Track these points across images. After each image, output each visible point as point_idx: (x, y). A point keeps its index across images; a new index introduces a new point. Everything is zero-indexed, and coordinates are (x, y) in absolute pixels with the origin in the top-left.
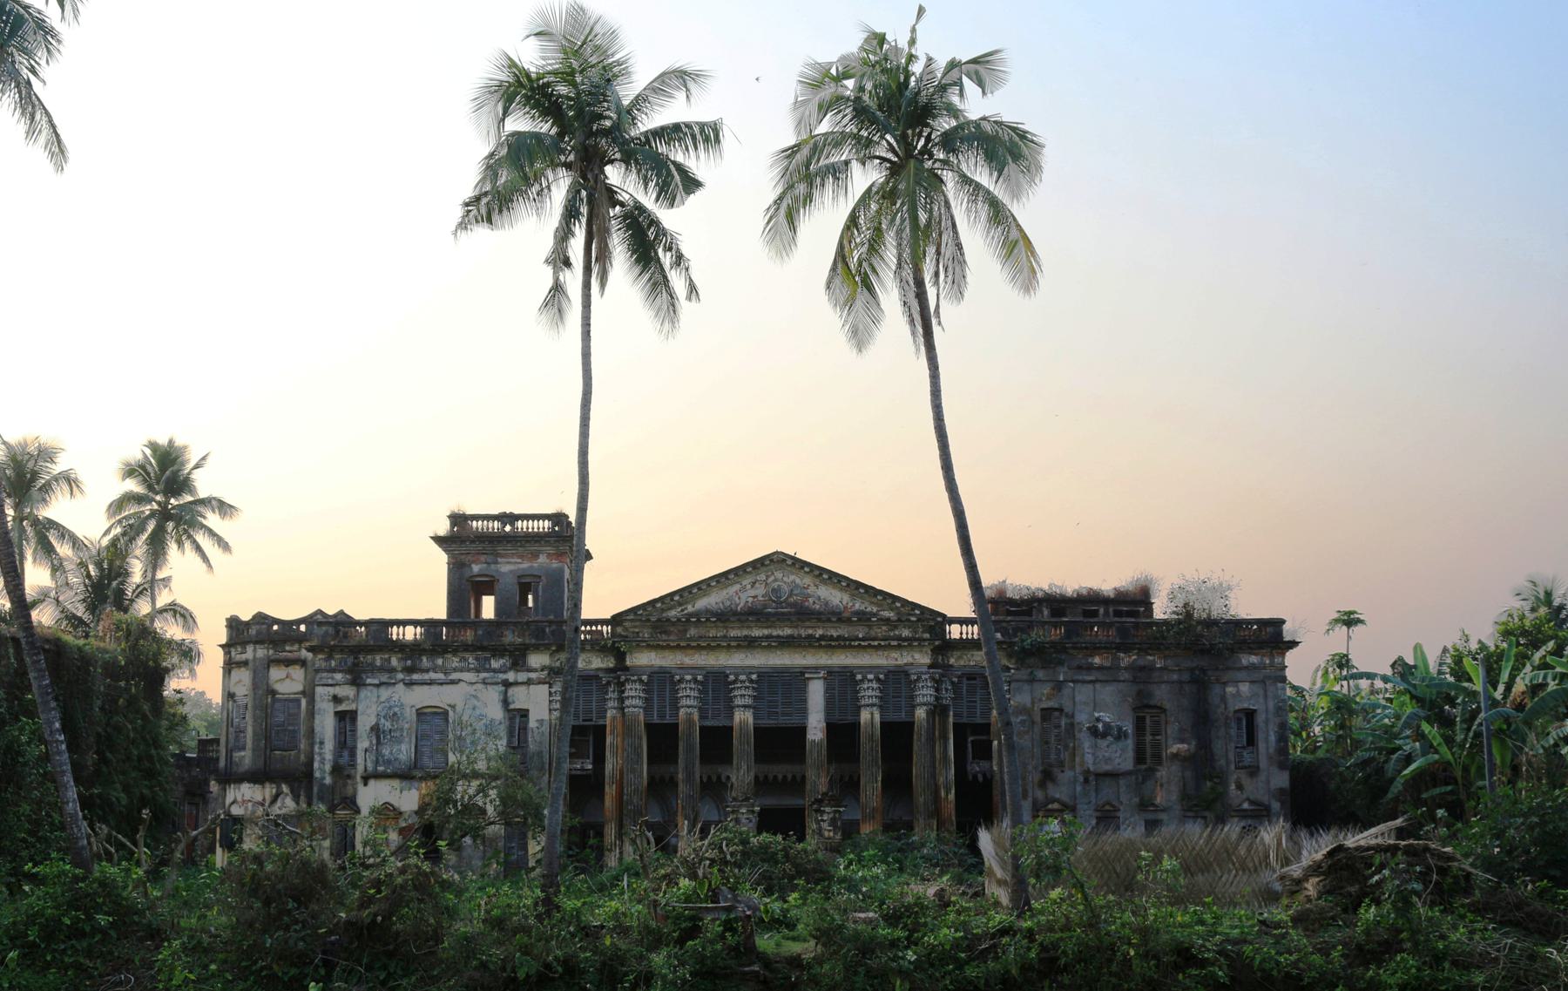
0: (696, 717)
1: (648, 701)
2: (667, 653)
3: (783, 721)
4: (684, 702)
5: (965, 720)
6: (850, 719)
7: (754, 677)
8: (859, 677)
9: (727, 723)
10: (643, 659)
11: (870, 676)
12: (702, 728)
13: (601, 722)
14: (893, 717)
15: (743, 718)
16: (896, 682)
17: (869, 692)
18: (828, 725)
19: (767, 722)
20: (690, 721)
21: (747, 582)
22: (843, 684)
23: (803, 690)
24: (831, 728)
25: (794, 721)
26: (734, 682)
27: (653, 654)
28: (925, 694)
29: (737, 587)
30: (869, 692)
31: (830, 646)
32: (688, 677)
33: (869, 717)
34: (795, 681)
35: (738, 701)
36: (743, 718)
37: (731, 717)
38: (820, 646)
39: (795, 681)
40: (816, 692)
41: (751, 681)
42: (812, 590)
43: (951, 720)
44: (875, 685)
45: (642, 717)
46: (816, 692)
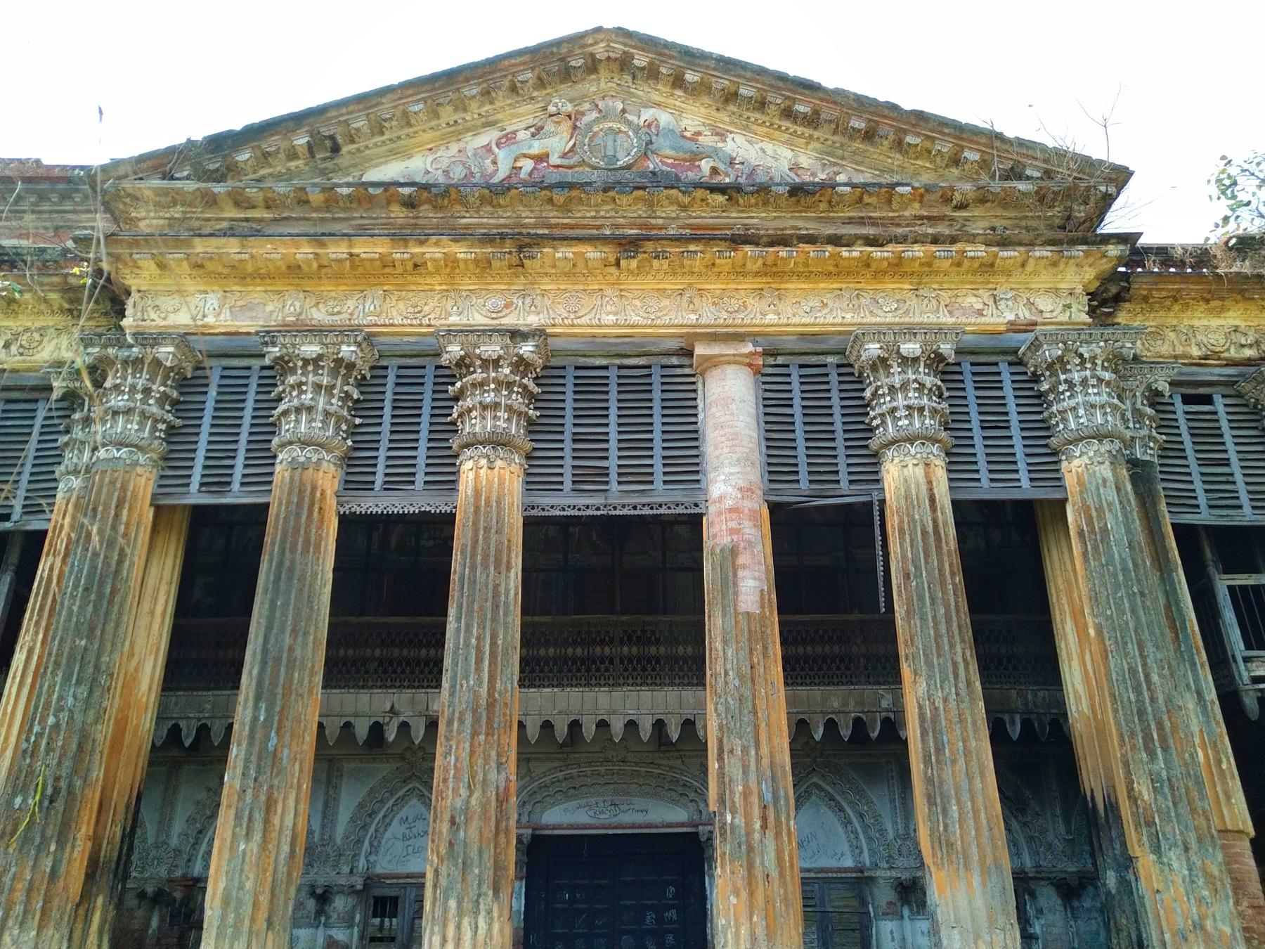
0: (329, 478)
1: (177, 441)
2: (256, 293)
3: (617, 499)
4: (287, 427)
5: (1205, 517)
6: (846, 492)
7: (527, 349)
8: (873, 349)
9: (433, 503)
10: (182, 306)
11: (911, 348)
12: (347, 521)
13: (35, 525)
14: (986, 488)
15: (490, 487)
16: (989, 383)
17: (904, 404)
18: (774, 508)
19: (565, 501)
20: (304, 496)
21: (520, 118)
22: (815, 390)
23: (683, 406)
24: (789, 525)
25: (662, 497)
26: (463, 364)
27: (213, 301)
28: (1085, 405)
29: (488, 137)
30: (904, 404)
31: (773, 272)
32: (311, 349)
33: (912, 480)
34: (657, 384)
35: (476, 425)
36: (490, 487)
37: (450, 485)
38: (739, 272)
39: (657, 384)
40: (729, 410)
41: (521, 365)
42: (707, 140)
43: (1167, 520)
44: (929, 381)
45: (144, 481)
46: (729, 410)
